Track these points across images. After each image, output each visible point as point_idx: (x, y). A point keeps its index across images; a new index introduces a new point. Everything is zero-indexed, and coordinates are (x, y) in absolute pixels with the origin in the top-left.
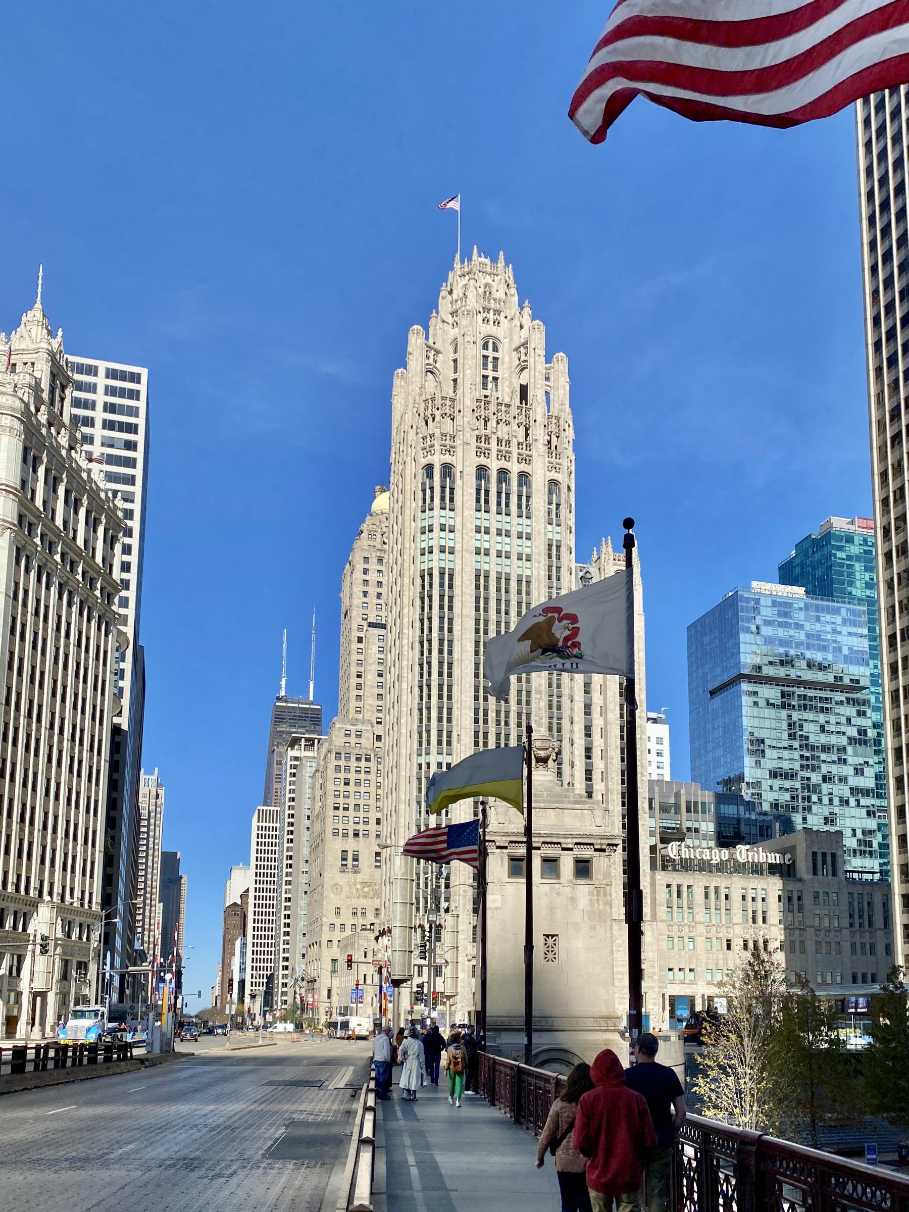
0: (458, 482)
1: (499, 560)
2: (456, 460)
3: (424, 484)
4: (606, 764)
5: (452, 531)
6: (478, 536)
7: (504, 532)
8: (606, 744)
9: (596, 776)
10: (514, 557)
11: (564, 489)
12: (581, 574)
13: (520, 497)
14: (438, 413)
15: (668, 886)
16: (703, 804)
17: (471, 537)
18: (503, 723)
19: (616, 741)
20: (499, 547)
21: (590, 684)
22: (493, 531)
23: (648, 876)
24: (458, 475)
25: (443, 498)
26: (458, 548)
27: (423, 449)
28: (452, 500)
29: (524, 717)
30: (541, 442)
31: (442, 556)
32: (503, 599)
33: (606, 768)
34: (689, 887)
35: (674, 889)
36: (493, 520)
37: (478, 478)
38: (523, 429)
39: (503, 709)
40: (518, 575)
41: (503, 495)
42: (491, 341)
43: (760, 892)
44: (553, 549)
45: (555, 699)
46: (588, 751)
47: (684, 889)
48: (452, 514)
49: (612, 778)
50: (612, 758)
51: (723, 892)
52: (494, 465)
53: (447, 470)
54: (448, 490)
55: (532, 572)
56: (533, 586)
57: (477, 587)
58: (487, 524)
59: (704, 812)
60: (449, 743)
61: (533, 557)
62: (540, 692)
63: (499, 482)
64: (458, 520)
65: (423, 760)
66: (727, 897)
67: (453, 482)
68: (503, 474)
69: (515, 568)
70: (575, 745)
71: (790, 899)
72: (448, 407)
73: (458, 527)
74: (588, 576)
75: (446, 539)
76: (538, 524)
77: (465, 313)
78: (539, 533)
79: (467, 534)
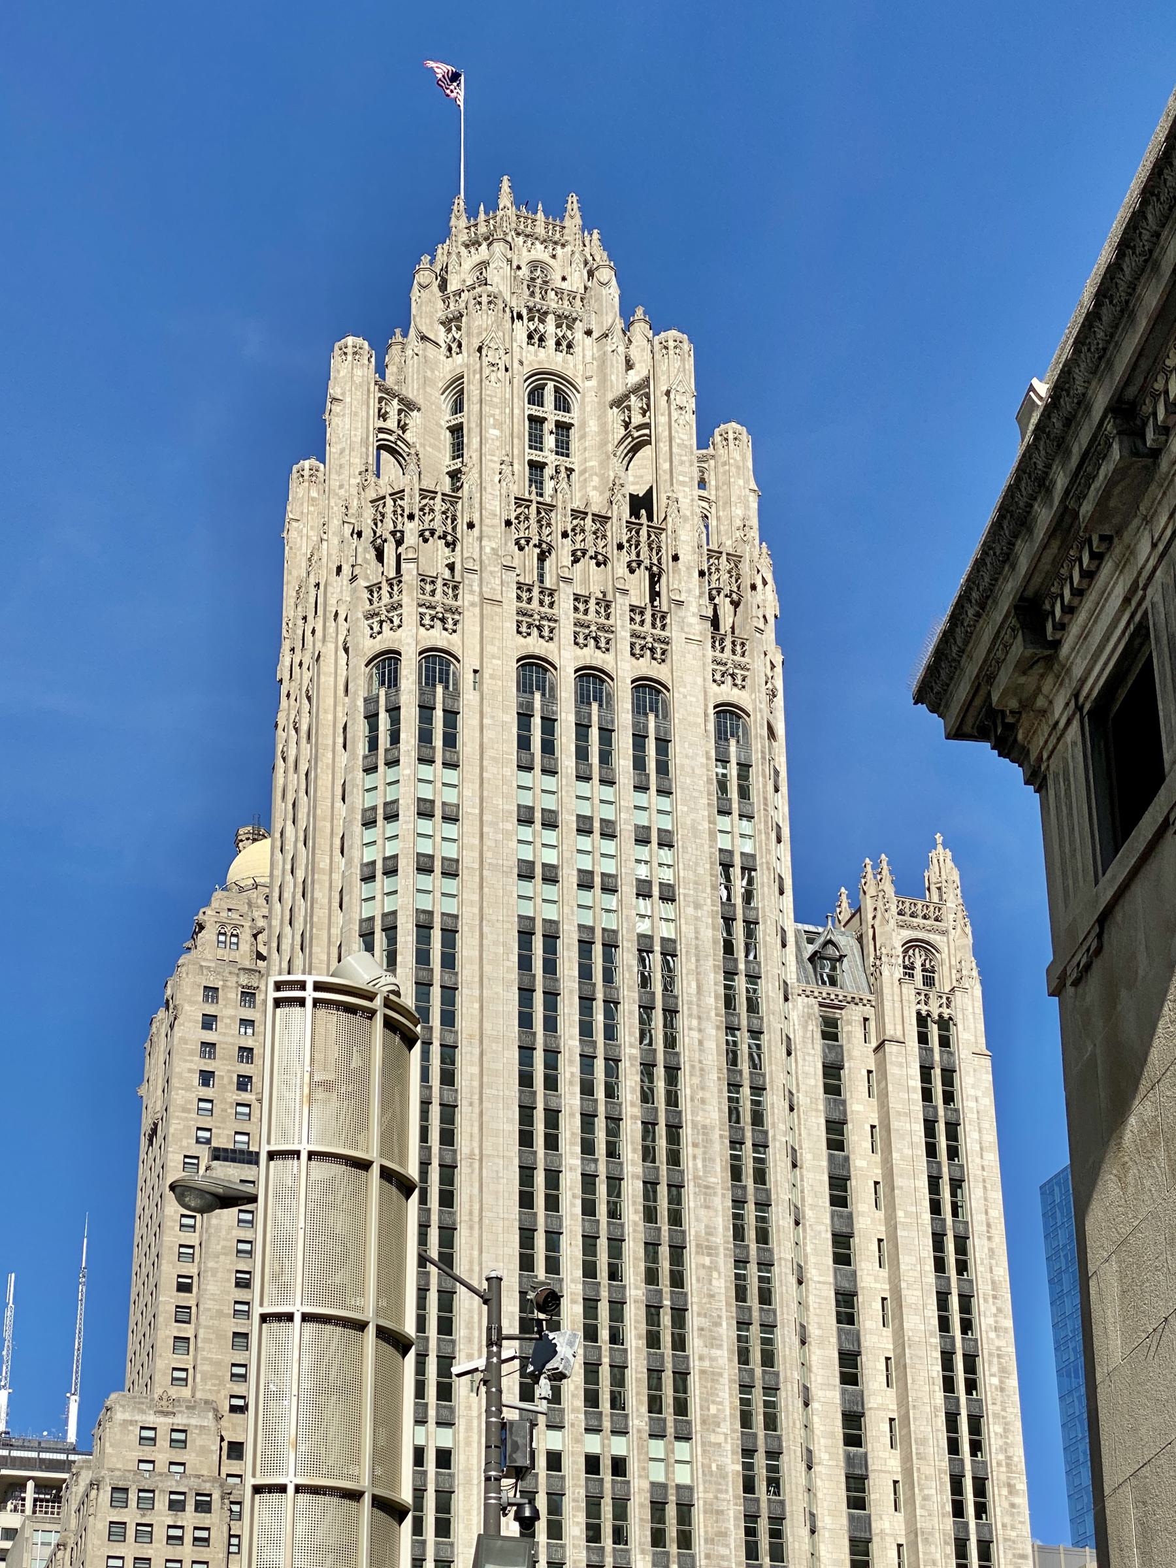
0: (469, 699)
1: (586, 897)
2: (464, 643)
4: (907, 1460)
5: (451, 818)
6: (526, 833)
7: (597, 825)
8: (903, 1401)
9: (879, 1492)
10: (628, 889)
12: (810, 949)
14: (411, 529)
17: (506, 833)
18: (604, 1334)
19: (931, 1393)
20: (586, 863)
21: (850, 1236)
22: (568, 821)
25: (425, 737)
26: (469, 861)
28: (450, 741)
29: (666, 1319)
30: (694, 608)
31: (425, 881)
32: (600, 996)
33: (908, 1471)
36: (568, 794)
38: (643, 575)
39: (604, 1294)
40: (641, 936)
41: (594, 733)
42: (551, 385)
45: (753, 1271)
46: (853, 1424)
48: (451, 776)
49: (926, 1498)
50: (923, 1442)
54: (439, 714)
55: (678, 930)
56: (684, 965)
58: (550, 803)
61: (681, 892)
62: (710, 1250)
64: (470, 792)
67: (453, 695)
68: (592, 681)
70: (815, 1405)
72: (439, 517)
73: (470, 810)
74: (830, 950)
77: (484, 299)
79: (494, 824)
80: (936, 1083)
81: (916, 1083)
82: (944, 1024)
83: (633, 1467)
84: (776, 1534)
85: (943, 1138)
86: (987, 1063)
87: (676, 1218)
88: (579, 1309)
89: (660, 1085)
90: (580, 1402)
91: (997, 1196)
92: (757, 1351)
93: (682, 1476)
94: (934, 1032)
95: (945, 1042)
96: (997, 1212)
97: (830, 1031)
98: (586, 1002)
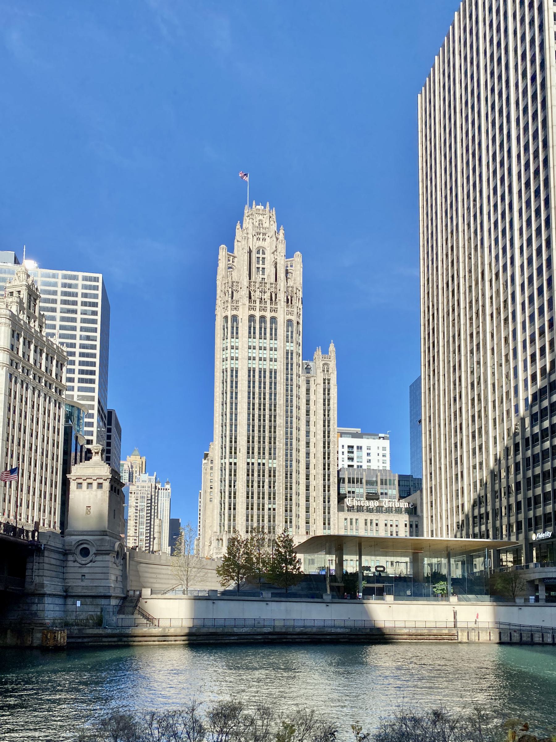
3: (224, 326)
11: (295, 324)
13: (271, 329)
15: (346, 519)
16: (390, 480)
23: (336, 515)
24: (240, 320)
27: (224, 308)
29: (273, 439)
30: (283, 300)
34: (357, 520)
35: (349, 520)
36: (256, 342)
37: (250, 321)
43: (394, 521)
44: (288, 354)
47: (354, 521)
51: (374, 522)
52: (258, 314)
53: (235, 318)
57: (249, 376)
59: (390, 484)
60: (235, 453)
61: (278, 360)
62: (280, 426)
63: (261, 322)
65: (223, 461)
66: (377, 525)
68: (263, 318)
69: (267, 366)
71: (411, 526)
74: (309, 367)
75: (234, 353)
76: (280, 343)
78: (281, 346)
80: (326, 391)
81: (322, 392)
82: (329, 380)
83: (266, 464)
84: (291, 474)
85: (326, 402)
86: (336, 387)
87: (275, 421)
88: (257, 438)
89: (273, 397)
90: (257, 454)
91: (336, 412)
92: (288, 444)
93: (275, 465)
94: (327, 381)
95: (329, 383)
96: (336, 416)
97: (308, 382)
98: (260, 382)
